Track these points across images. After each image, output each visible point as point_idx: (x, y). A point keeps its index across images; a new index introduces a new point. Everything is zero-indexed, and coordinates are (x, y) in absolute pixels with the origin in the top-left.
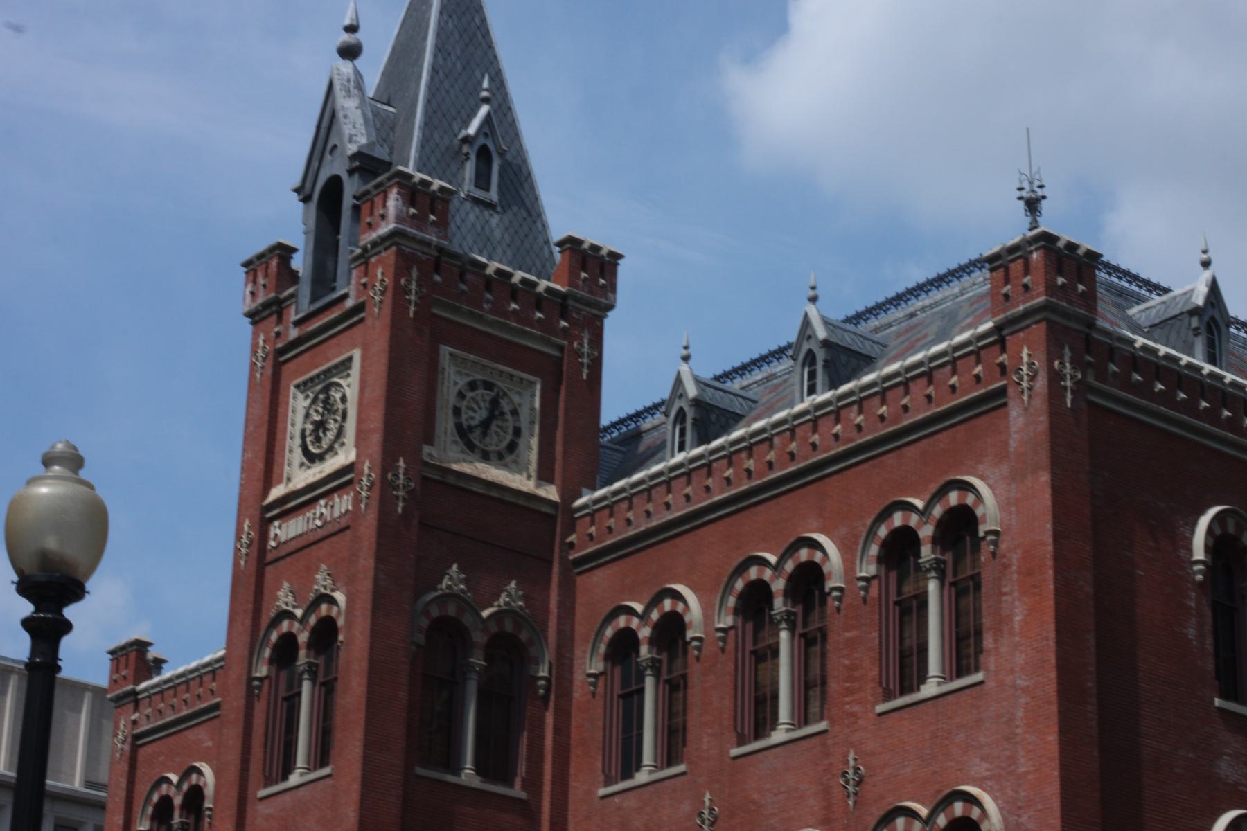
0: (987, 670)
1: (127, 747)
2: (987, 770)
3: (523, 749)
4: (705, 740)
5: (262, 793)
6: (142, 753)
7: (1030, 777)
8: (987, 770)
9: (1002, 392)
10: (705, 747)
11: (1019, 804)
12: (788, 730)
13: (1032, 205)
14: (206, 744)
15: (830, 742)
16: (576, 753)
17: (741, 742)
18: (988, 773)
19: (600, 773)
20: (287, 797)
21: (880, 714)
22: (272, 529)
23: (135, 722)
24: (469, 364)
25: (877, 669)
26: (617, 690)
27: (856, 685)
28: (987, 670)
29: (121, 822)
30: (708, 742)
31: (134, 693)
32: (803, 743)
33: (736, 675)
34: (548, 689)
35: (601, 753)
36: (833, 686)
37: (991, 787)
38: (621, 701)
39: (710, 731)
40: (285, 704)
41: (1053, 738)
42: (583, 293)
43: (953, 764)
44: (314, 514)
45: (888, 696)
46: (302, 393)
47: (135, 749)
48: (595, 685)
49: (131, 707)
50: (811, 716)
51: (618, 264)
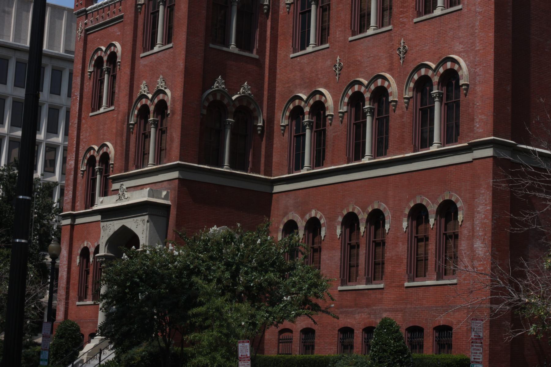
0: (463, 4)
1: (83, 35)
2: (462, 48)
3: (257, 37)
4: (338, 33)
5: (142, 55)
6: (89, 37)
7: (481, 51)
8: (462, 48)
10: (337, 36)
11: (476, 64)
12: (374, 29)
14: (117, 34)
15: (393, 35)
16: (280, 38)
17: (353, 35)
18: (462, 49)
19: (291, 47)
20: (153, 56)
21: (415, 23)
23: (86, 24)
25: (415, 3)
26: (299, 11)
27: (405, 10)
28: (463, 4)
29: (81, 68)
30: (339, 34)
31: (86, 11)
32: (381, 35)
33: (352, 4)
34: (268, 10)
35: (291, 38)
36: (395, 10)
37: (463, 55)
38: (301, 15)
39: (340, 29)
40: (152, 15)
41: (492, 34)
43: (447, 45)
45: (419, 15)
47: (86, 36)
48: (289, 8)
49: (84, 17)
50: (385, 23)
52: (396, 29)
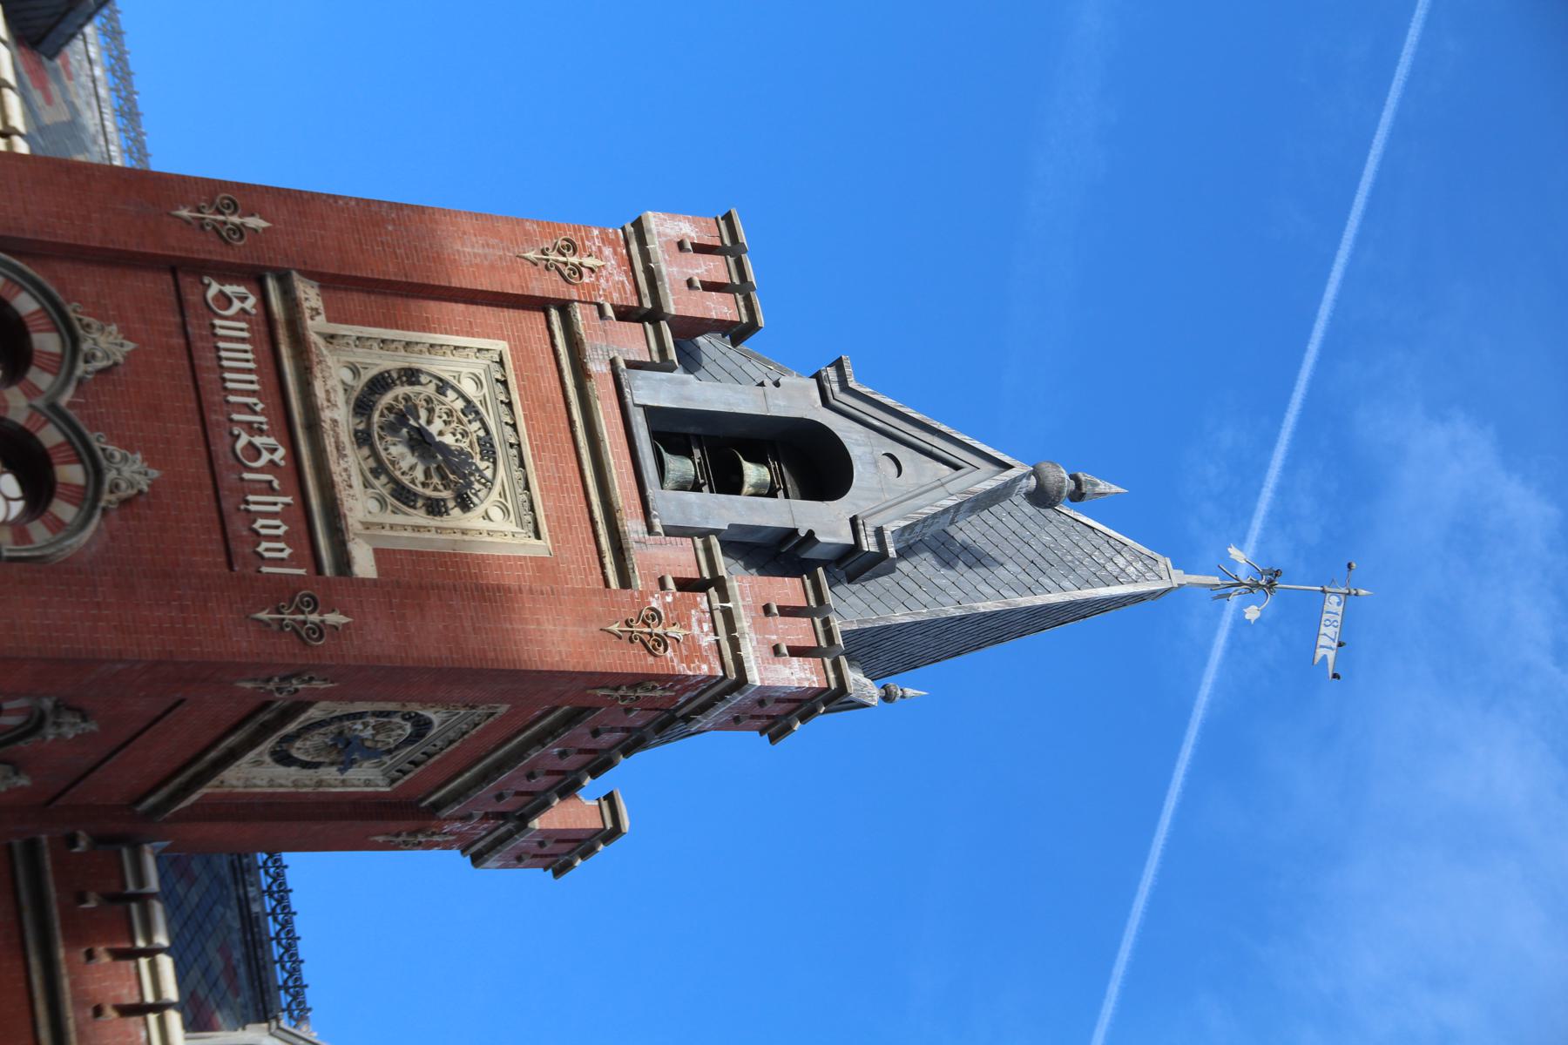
22: (242, 290)
24: (465, 726)
42: (517, 842)
44: (261, 432)
46: (488, 370)
51: (546, 869)
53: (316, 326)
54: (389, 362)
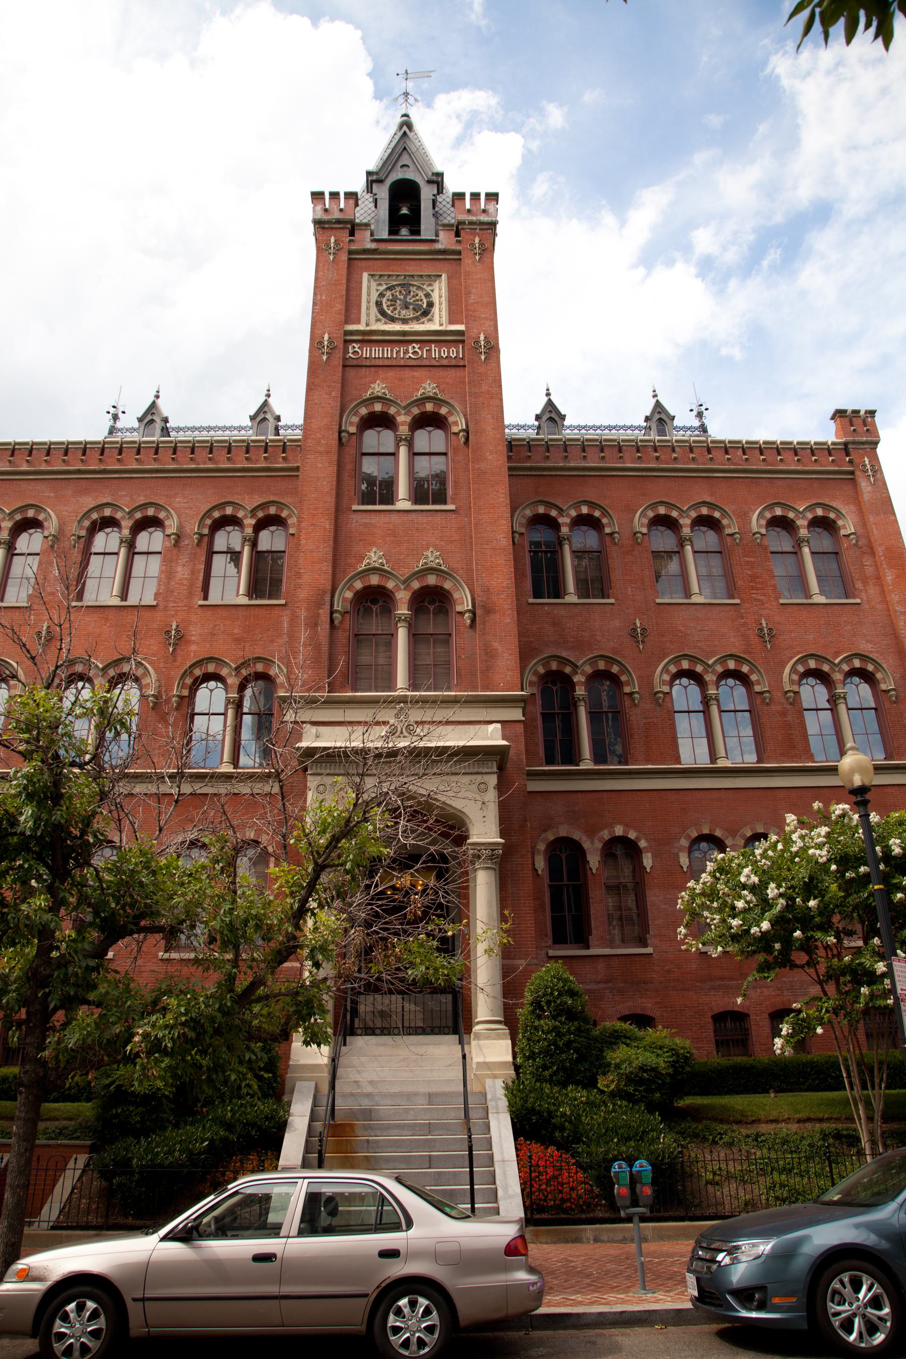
9: (852, 473)
13: (700, 415)
46: (375, 281)
52: (747, 605)
53: (361, 327)
54: (374, 310)
